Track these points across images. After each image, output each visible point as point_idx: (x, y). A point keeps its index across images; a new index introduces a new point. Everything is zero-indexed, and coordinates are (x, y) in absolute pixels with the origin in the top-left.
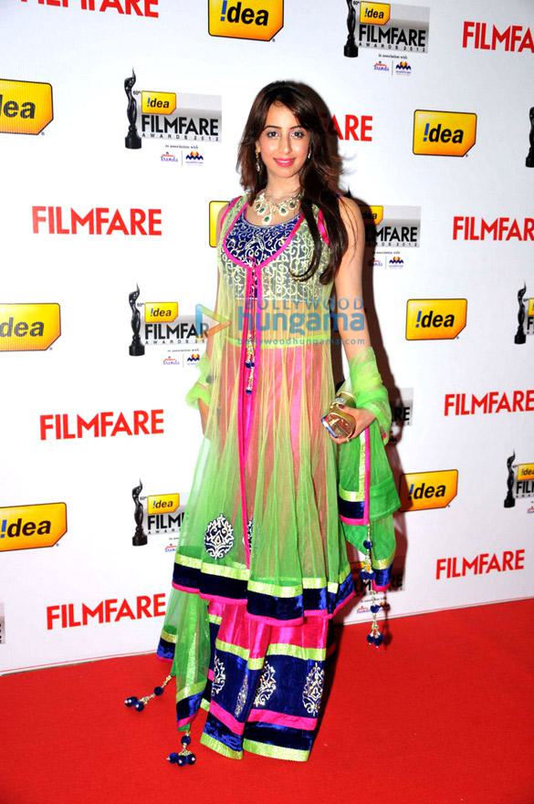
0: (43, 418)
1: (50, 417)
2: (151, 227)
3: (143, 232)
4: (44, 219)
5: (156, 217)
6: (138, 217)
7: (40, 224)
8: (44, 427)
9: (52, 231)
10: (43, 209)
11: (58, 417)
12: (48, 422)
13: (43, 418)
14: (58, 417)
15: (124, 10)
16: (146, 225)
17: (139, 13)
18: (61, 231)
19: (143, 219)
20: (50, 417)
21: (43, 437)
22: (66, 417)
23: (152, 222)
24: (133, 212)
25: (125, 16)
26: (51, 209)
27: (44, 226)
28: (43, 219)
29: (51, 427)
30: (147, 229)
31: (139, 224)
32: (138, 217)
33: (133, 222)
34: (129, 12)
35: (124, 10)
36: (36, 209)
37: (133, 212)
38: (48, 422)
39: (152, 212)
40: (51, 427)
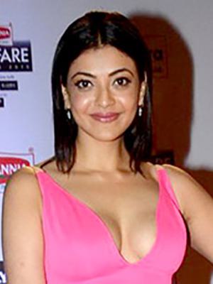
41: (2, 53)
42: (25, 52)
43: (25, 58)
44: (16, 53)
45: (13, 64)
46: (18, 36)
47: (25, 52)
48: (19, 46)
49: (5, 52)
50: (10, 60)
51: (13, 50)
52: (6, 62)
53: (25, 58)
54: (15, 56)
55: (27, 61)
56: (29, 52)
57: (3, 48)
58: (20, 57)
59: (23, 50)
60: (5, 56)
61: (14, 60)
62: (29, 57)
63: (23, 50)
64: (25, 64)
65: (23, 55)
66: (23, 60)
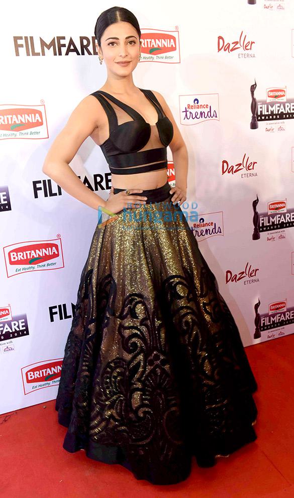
0: (51, 309)
1: (55, 307)
2: (107, 184)
3: (103, 188)
4: (40, 189)
5: (109, 177)
6: (99, 179)
7: (38, 192)
8: (52, 314)
9: (46, 195)
10: (39, 182)
11: (60, 306)
12: (54, 310)
13: (51, 309)
14: (60, 306)
15: (80, 53)
16: (104, 184)
17: (89, 53)
18: (52, 195)
19: (102, 180)
20: (55, 307)
21: (52, 320)
22: (64, 305)
23: (108, 181)
24: (96, 176)
25: (81, 56)
26: (44, 181)
27: (41, 193)
28: (40, 189)
29: (56, 313)
30: (105, 187)
31: (100, 183)
32: (99, 179)
33: (96, 183)
34: (83, 54)
35: (80, 53)
36: (35, 183)
37: (96, 176)
38: (54, 310)
39: (107, 175)
40: (56, 313)
41: (3, 327)
42: (22, 323)
43: (23, 326)
44: (15, 324)
45: (13, 333)
46: (15, 312)
47: (22, 323)
48: (17, 319)
49: (6, 326)
50: (11, 331)
51: (13, 323)
52: (8, 333)
53: (23, 326)
54: (13, 327)
55: (24, 328)
56: (26, 322)
57: (4, 323)
58: (18, 327)
59: (20, 321)
60: (7, 329)
61: (14, 330)
62: (26, 326)
63: (20, 321)
64: (23, 331)
65: (21, 325)
66: (21, 329)
